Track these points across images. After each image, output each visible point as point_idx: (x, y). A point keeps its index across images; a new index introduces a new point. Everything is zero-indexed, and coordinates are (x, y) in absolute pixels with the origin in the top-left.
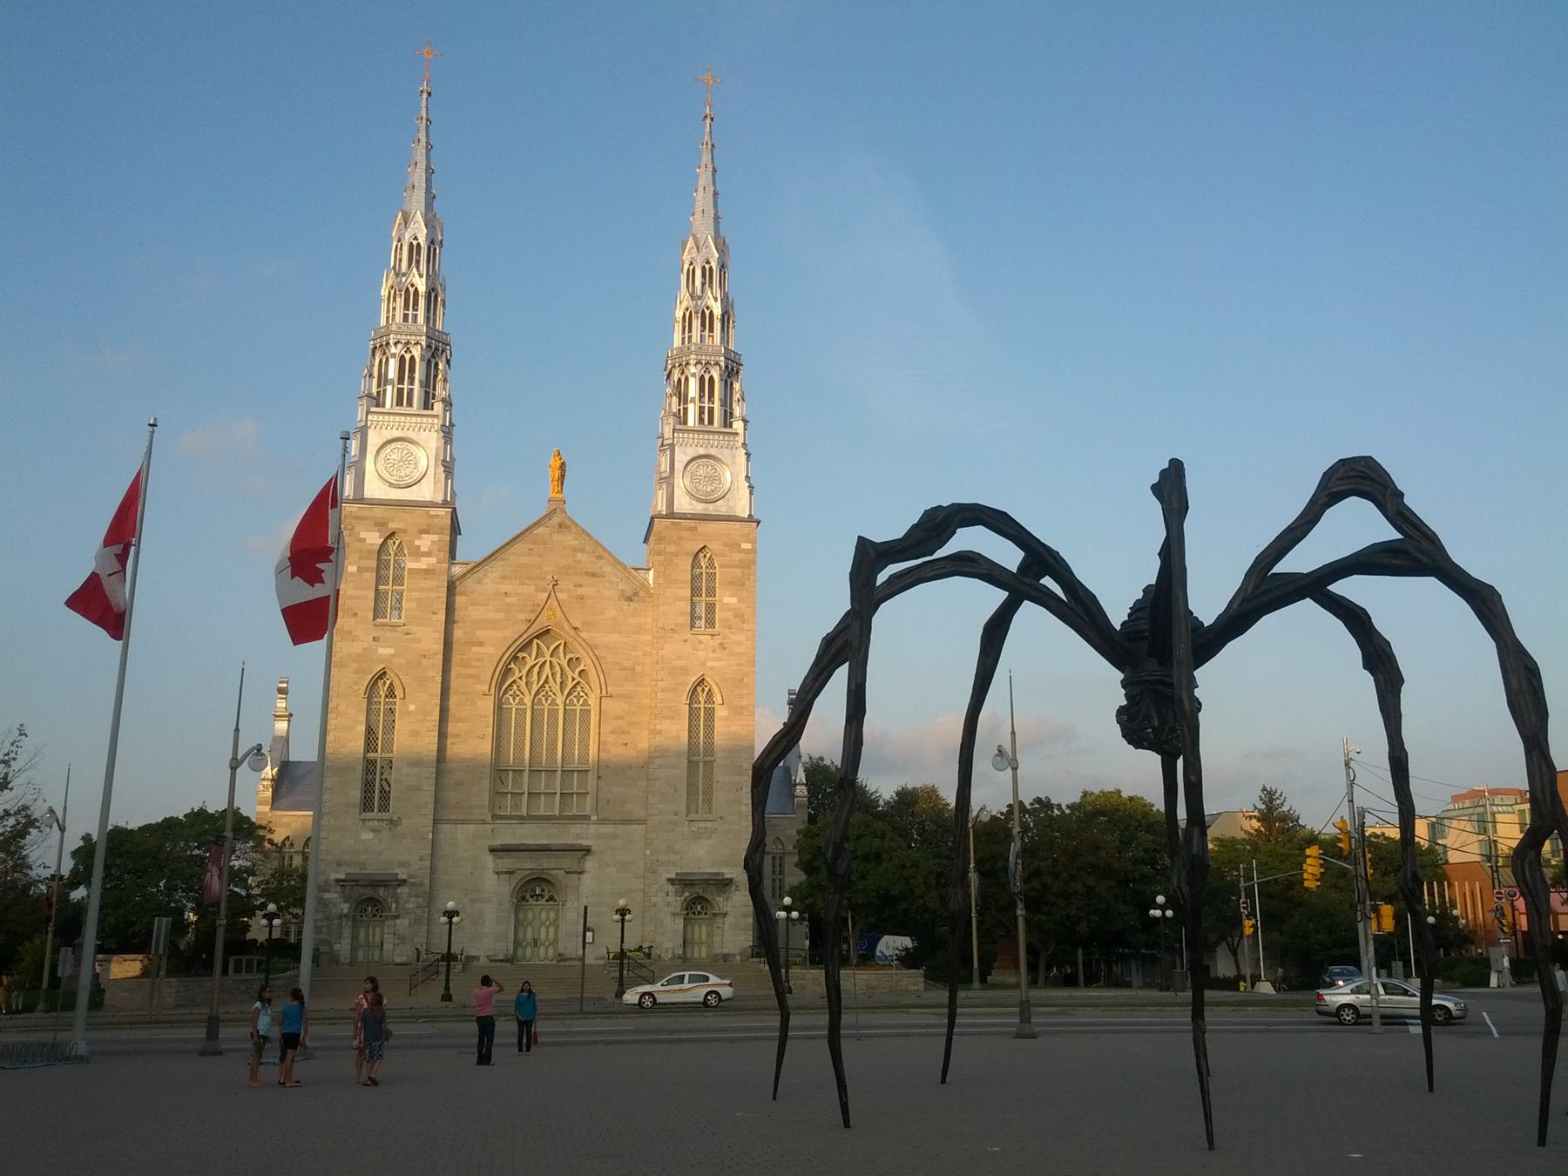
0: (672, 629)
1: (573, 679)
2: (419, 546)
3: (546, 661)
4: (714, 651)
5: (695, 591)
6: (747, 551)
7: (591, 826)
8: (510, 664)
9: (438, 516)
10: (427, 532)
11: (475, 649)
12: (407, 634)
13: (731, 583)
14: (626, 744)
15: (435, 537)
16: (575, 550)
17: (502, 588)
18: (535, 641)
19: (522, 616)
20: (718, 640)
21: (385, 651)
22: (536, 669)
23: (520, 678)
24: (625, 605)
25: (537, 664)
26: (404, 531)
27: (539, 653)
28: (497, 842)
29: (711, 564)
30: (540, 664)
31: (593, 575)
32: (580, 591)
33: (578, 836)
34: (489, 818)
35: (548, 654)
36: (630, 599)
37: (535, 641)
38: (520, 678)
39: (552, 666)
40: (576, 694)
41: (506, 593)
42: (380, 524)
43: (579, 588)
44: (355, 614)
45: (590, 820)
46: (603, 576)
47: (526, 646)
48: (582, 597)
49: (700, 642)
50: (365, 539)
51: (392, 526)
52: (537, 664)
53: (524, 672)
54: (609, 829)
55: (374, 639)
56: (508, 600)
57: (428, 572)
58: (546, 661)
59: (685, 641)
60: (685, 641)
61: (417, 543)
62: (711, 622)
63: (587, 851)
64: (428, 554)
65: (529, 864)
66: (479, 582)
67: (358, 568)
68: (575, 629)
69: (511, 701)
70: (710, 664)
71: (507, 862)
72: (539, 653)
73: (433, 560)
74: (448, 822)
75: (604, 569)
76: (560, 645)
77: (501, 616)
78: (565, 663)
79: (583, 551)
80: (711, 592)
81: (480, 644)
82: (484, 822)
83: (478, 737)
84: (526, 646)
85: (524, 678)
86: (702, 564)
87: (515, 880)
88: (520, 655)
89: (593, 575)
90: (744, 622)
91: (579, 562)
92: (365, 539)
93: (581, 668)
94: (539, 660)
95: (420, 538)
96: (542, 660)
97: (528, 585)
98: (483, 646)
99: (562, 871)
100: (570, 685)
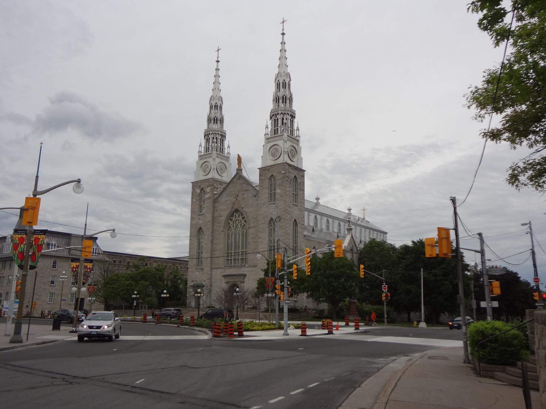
0: (264, 204)
1: (243, 223)
4: (274, 209)
5: (271, 190)
6: (284, 174)
8: (228, 221)
9: (211, 182)
11: (221, 218)
12: (205, 216)
13: (279, 185)
14: (255, 242)
15: (210, 188)
16: (242, 184)
17: (226, 199)
18: (234, 213)
19: (231, 206)
20: (275, 205)
21: (201, 222)
22: (235, 221)
23: (231, 225)
24: (254, 198)
26: (204, 187)
27: (236, 217)
28: (225, 274)
29: (275, 181)
31: (247, 191)
32: (244, 196)
33: (243, 271)
34: (223, 267)
35: (237, 216)
36: (255, 196)
37: (234, 213)
38: (231, 225)
40: (244, 228)
41: (227, 200)
42: (200, 187)
43: (243, 195)
44: (195, 213)
45: (246, 266)
46: (249, 190)
47: (232, 215)
48: (244, 198)
49: (271, 207)
50: (197, 192)
51: (202, 186)
53: (232, 223)
54: (251, 269)
55: (199, 219)
56: (228, 202)
57: (209, 198)
59: (267, 207)
60: (267, 207)
62: (275, 200)
63: (245, 275)
64: (209, 193)
65: (232, 280)
66: (221, 198)
67: (196, 200)
68: (243, 208)
69: (230, 232)
70: (273, 213)
71: (228, 280)
72: (236, 217)
73: (210, 194)
74: (215, 268)
75: (249, 188)
76: (240, 214)
77: (225, 207)
79: (244, 183)
80: (275, 190)
81: (222, 216)
82: (222, 268)
84: (232, 215)
86: (273, 181)
87: (229, 284)
88: (231, 218)
89: (247, 191)
90: (282, 197)
91: (243, 187)
92: (197, 192)
93: (245, 220)
95: (207, 189)
96: (236, 219)
98: (222, 217)
100: (242, 225)
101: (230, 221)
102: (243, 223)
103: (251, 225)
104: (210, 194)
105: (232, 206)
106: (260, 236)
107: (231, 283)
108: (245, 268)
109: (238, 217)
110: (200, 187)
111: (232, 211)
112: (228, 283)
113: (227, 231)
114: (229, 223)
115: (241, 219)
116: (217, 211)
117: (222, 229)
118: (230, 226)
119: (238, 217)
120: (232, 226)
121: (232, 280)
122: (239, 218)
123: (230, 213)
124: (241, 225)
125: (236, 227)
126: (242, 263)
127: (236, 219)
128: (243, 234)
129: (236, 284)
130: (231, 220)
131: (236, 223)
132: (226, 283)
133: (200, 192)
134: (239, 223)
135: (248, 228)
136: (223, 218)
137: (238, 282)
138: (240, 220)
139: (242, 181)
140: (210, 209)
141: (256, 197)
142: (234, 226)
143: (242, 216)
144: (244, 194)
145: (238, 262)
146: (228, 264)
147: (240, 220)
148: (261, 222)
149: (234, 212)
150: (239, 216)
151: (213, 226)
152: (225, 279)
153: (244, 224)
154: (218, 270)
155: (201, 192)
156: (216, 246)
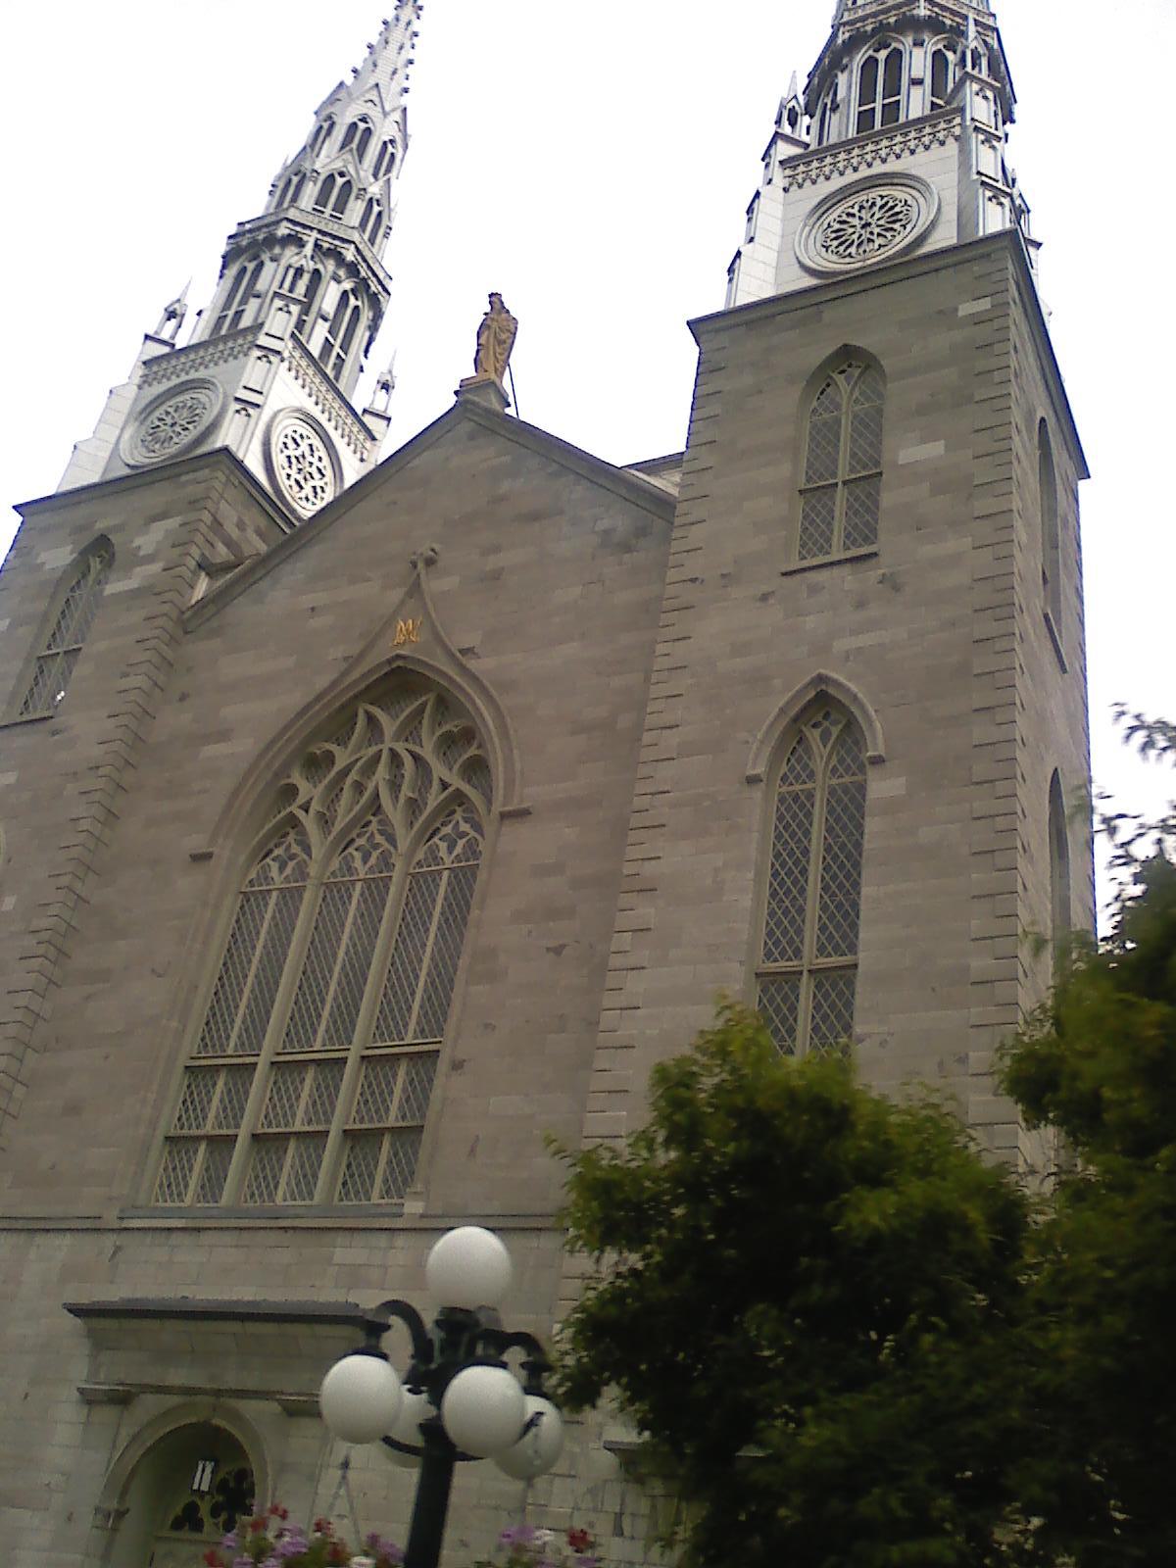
1: (445, 786)
2: (139, 547)
3: (377, 757)
7: (400, 1240)
10: (163, 516)
14: (558, 951)
17: (306, 601)
19: (338, 652)
22: (353, 776)
25: (357, 760)
26: (119, 528)
30: (364, 760)
39: (394, 755)
41: (313, 609)
48: (496, 576)
51: (101, 526)
52: (357, 760)
56: (316, 623)
58: (377, 757)
61: (137, 542)
64: (150, 559)
73: (156, 568)
76: (424, 705)
78: (427, 752)
83: (153, 971)
85: (315, 806)
93: (472, 751)
94: (363, 752)
96: (373, 750)
97: (368, 580)
99: (274, 1407)
100: (434, 799)
101: (297, 778)
102: (445, 786)
103: (531, 794)
104: (156, 568)
105: (355, 650)
106: (649, 868)
107: (148, 1406)
108: (382, 1240)
109: (397, 738)
110: (79, 529)
111: (349, 680)
112: (122, 1399)
113: (242, 858)
114: (291, 791)
115: (427, 752)
116: (183, 698)
117: (197, 842)
118: (293, 822)
119: (397, 738)
120: (309, 822)
121: (177, 1377)
122: (400, 747)
123: (318, 698)
124: (414, 806)
125: (360, 823)
126: (354, 1181)
127: (373, 750)
128: (421, 884)
129: (218, 1430)
130: (316, 764)
131: (359, 787)
132: (89, 1399)
133: (74, 564)
134: (395, 786)
135: (504, 816)
136: (244, 746)
137: (250, 1408)
138: (416, 758)
139: (489, 454)
140: (126, 675)
141: (627, 556)
142: (341, 811)
143: (437, 723)
144: (496, 549)
145: (306, 1182)
146: (173, 1186)
147: (416, 758)
148: (673, 738)
149: (356, 697)
150: (409, 730)
151: (111, 817)
152: (99, 1344)
153: (459, 798)
154: (40, 1239)
155: (80, 568)
156: (88, 998)
